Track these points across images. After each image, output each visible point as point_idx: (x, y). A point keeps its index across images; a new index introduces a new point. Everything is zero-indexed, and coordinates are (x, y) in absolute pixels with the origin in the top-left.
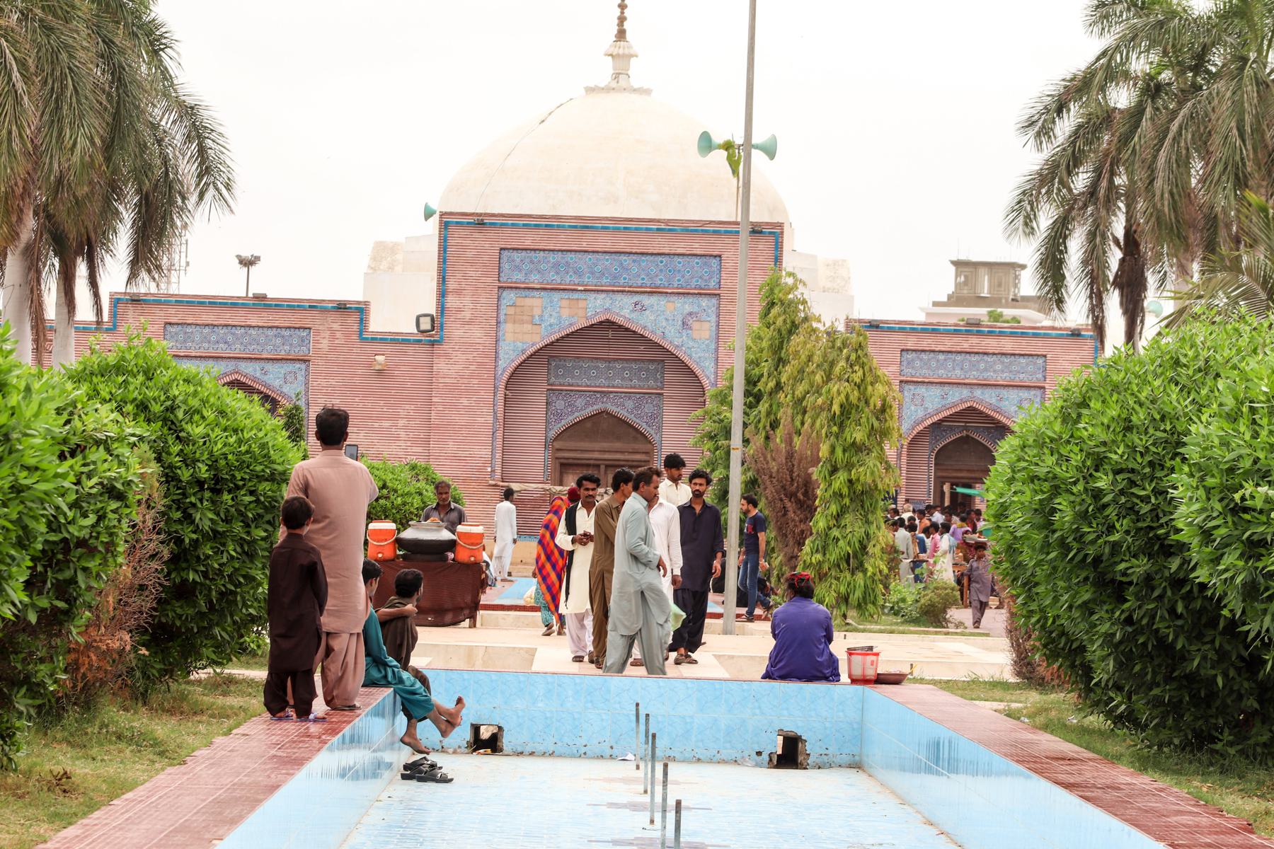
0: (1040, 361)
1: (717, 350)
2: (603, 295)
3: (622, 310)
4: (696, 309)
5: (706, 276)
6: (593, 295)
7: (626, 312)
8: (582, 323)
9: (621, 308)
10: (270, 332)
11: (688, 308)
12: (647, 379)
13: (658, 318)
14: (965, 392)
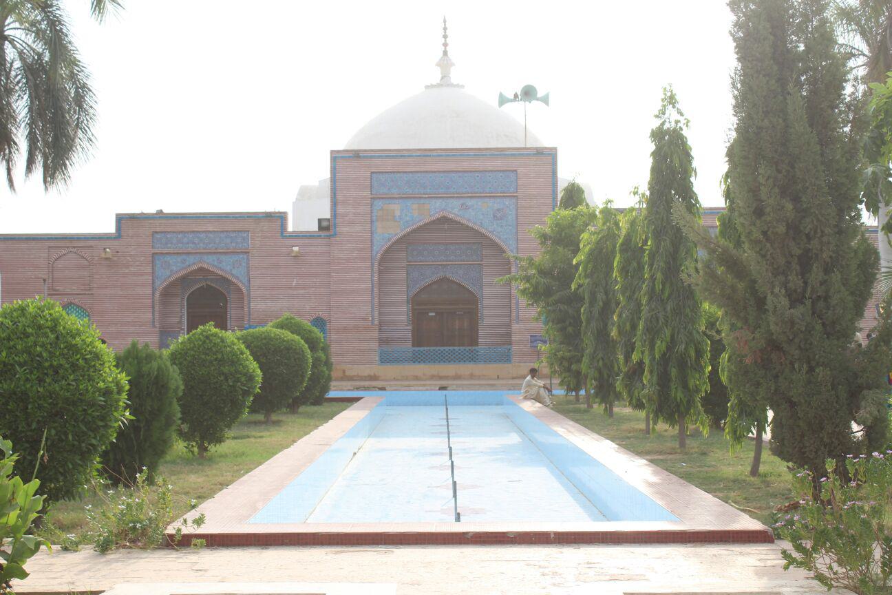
1: (517, 233)
3: (454, 209)
7: (456, 211)
8: (428, 220)
10: (222, 235)
11: (496, 206)
13: (477, 214)
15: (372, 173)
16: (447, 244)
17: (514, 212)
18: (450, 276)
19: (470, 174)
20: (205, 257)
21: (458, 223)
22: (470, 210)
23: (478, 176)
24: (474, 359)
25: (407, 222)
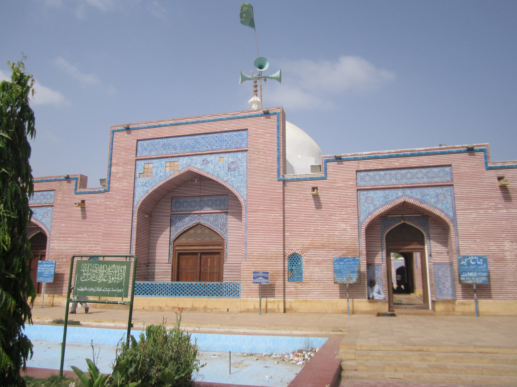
0: (447, 169)
2: (187, 158)
3: (197, 165)
4: (235, 160)
5: (240, 142)
6: (182, 158)
7: (198, 166)
9: (196, 164)
11: (231, 160)
12: (220, 205)
14: (400, 193)
15: (138, 140)
16: (200, 196)
18: (202, 222)
19: (211, 135)
21: (210, 180)
22: (210, 164)
23: (216, 137)
24: (209, 293)
25: (161, 177)
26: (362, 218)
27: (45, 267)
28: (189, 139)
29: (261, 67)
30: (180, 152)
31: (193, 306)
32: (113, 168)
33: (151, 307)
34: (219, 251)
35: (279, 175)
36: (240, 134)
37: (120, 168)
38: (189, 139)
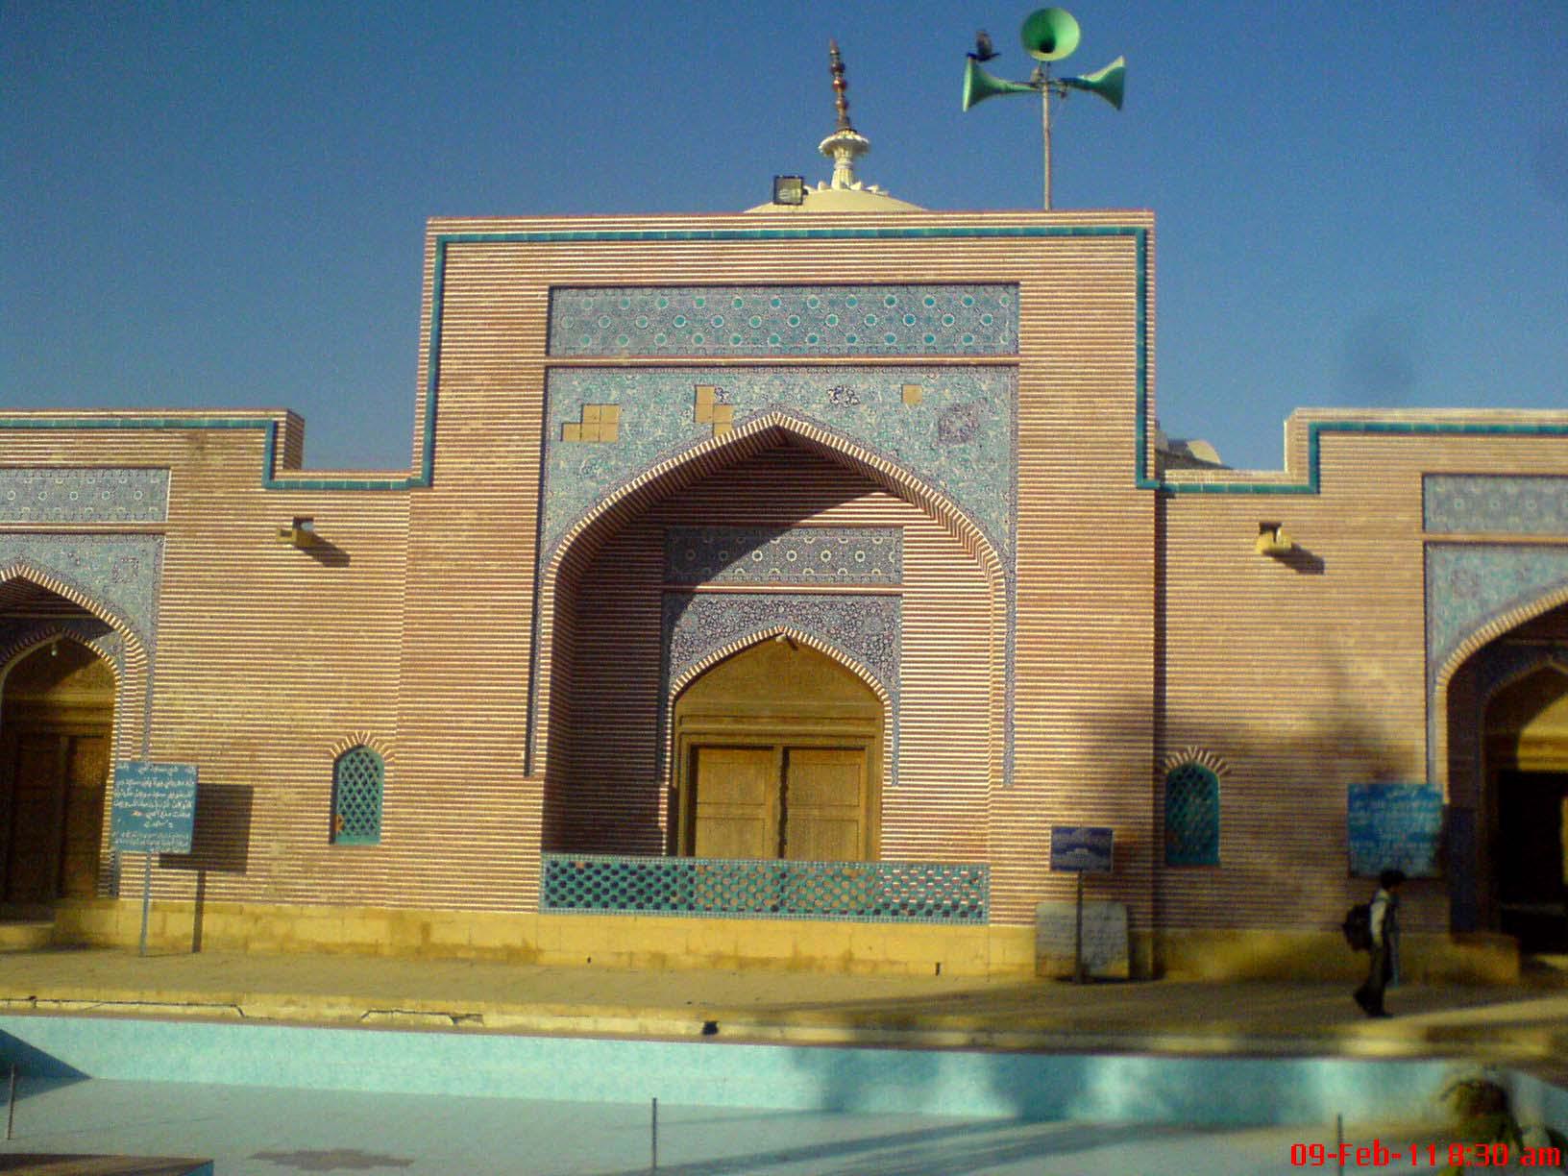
1: (1013, 483)
2: (767, 376)
4: (967, 398)
6: (746, 376)
7: (816, 410)
10: (88, 479)
11: (949, 397)
15: (552, 289)
17: (1005, 417)
20: (34, 545)
22: (862, 408)
23: (891, 302)
25: (656, 443)
26: (1438, 645)
27: (147, 790)
28: (775, 303)
29: (1048, 46)
30: (736, 348)
31: (796, 952)
32: (444, 394)
33: (619, 954)
34: (861, 743)
35: (1143, 469)
36: (986, 302)
37: (478, 399)
38: (775, 303)
